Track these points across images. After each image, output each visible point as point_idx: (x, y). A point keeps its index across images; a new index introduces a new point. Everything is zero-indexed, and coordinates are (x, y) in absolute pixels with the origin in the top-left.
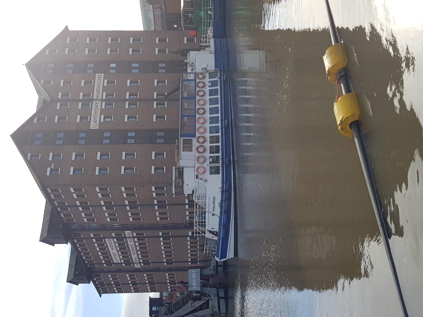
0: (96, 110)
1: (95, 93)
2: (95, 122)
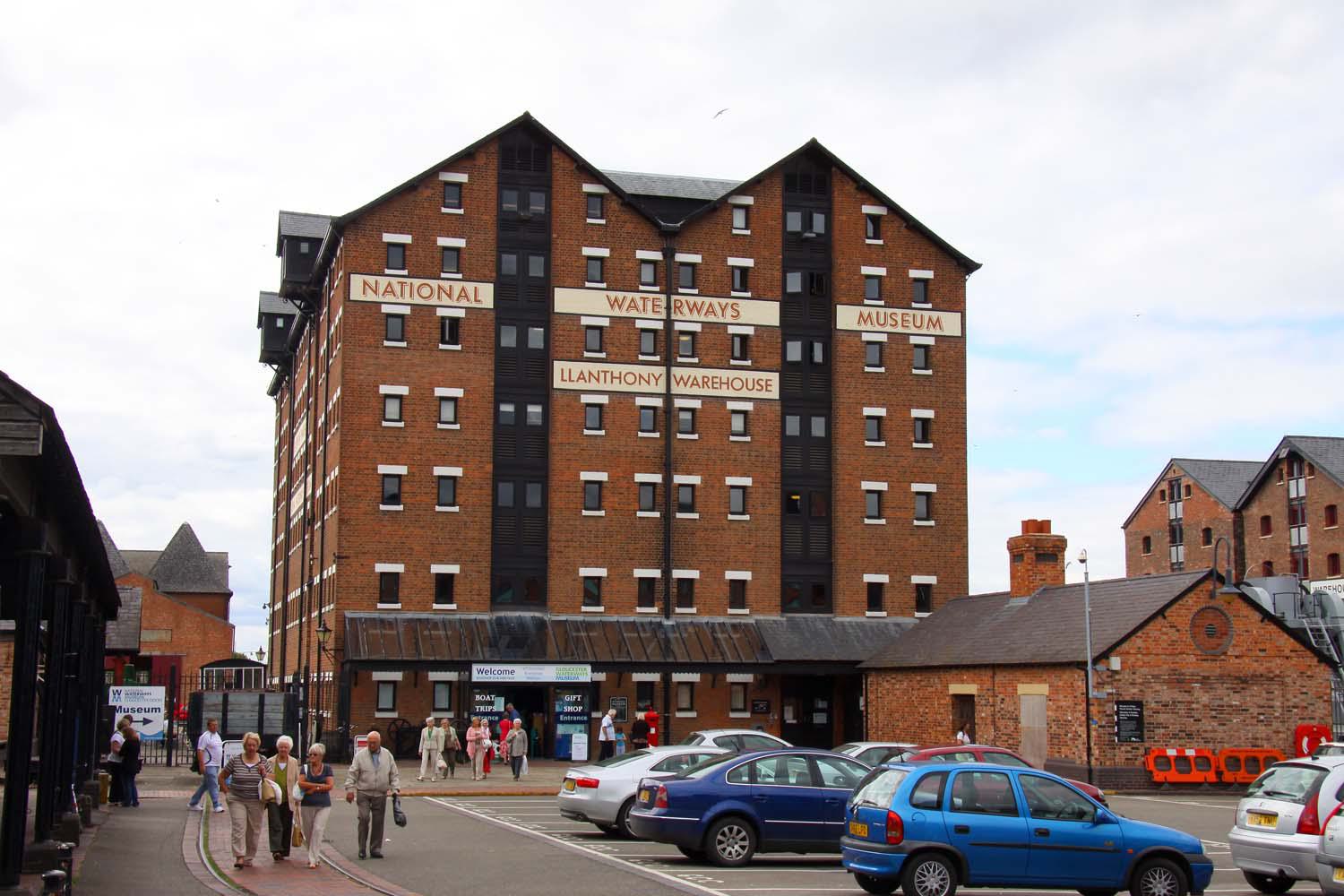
0: (630, 379)
1: (699, 373)
2: (581, 377)
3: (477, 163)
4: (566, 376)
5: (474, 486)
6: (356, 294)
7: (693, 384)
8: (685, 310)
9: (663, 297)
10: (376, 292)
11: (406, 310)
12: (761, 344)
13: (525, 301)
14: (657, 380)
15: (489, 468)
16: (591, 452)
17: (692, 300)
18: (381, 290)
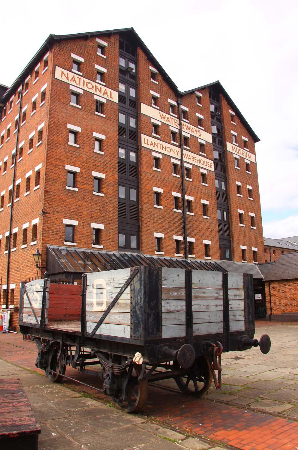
1: (191, 154)
2: (151, 144)
3: (110, 40)
4: (146, 142)
5: (110, 185)
6: (58, 76)
7: (189, 158)
8: (185, 127)
9: (178, 120)
10: (67, 78)
11: (81, 92)
12: (208, 149)
13: (130, 105)
14: (178, 153)
15: (117, 177)
16: (156, 179)
17: (187, 124)
18: (70, 78)
